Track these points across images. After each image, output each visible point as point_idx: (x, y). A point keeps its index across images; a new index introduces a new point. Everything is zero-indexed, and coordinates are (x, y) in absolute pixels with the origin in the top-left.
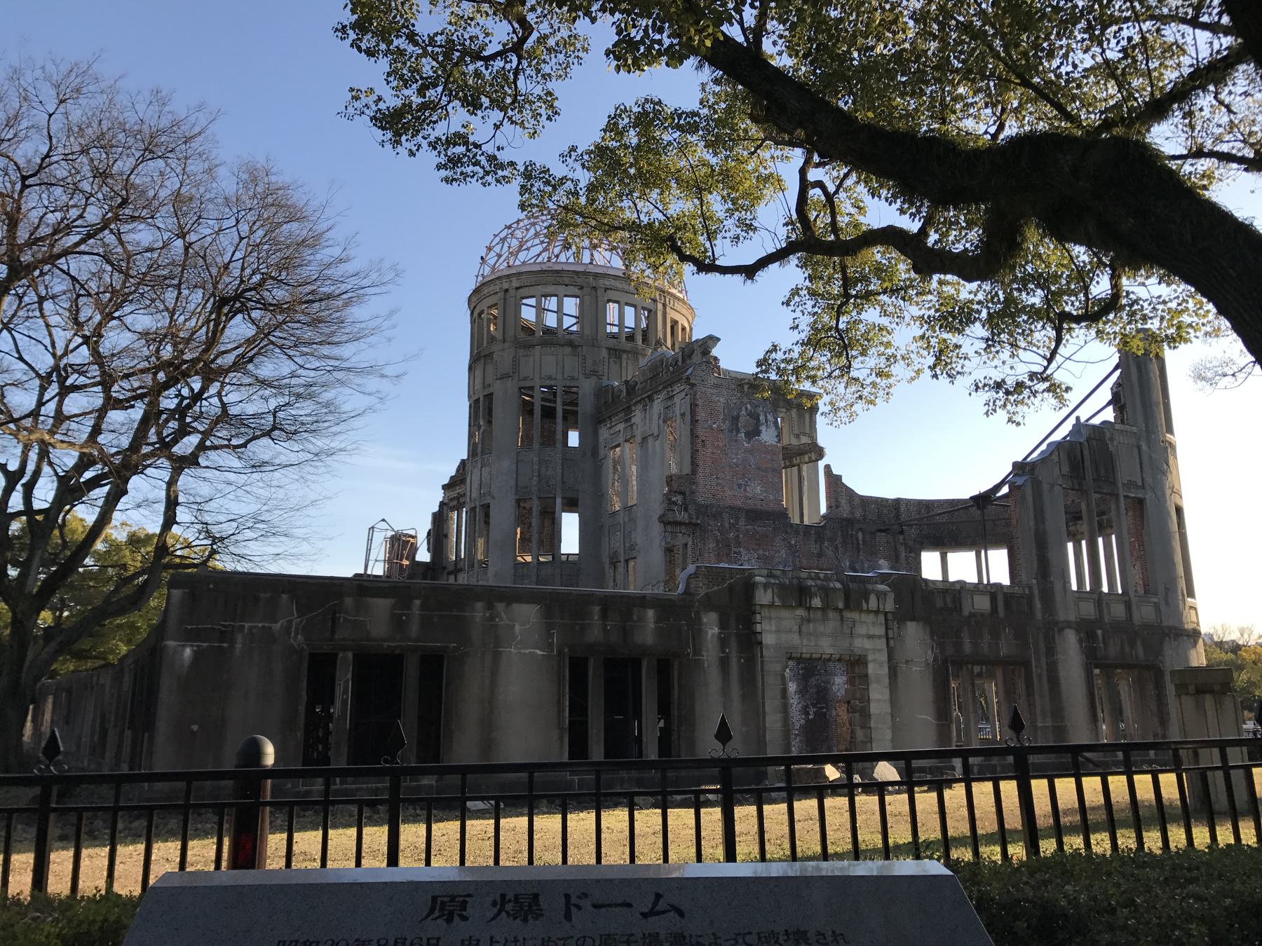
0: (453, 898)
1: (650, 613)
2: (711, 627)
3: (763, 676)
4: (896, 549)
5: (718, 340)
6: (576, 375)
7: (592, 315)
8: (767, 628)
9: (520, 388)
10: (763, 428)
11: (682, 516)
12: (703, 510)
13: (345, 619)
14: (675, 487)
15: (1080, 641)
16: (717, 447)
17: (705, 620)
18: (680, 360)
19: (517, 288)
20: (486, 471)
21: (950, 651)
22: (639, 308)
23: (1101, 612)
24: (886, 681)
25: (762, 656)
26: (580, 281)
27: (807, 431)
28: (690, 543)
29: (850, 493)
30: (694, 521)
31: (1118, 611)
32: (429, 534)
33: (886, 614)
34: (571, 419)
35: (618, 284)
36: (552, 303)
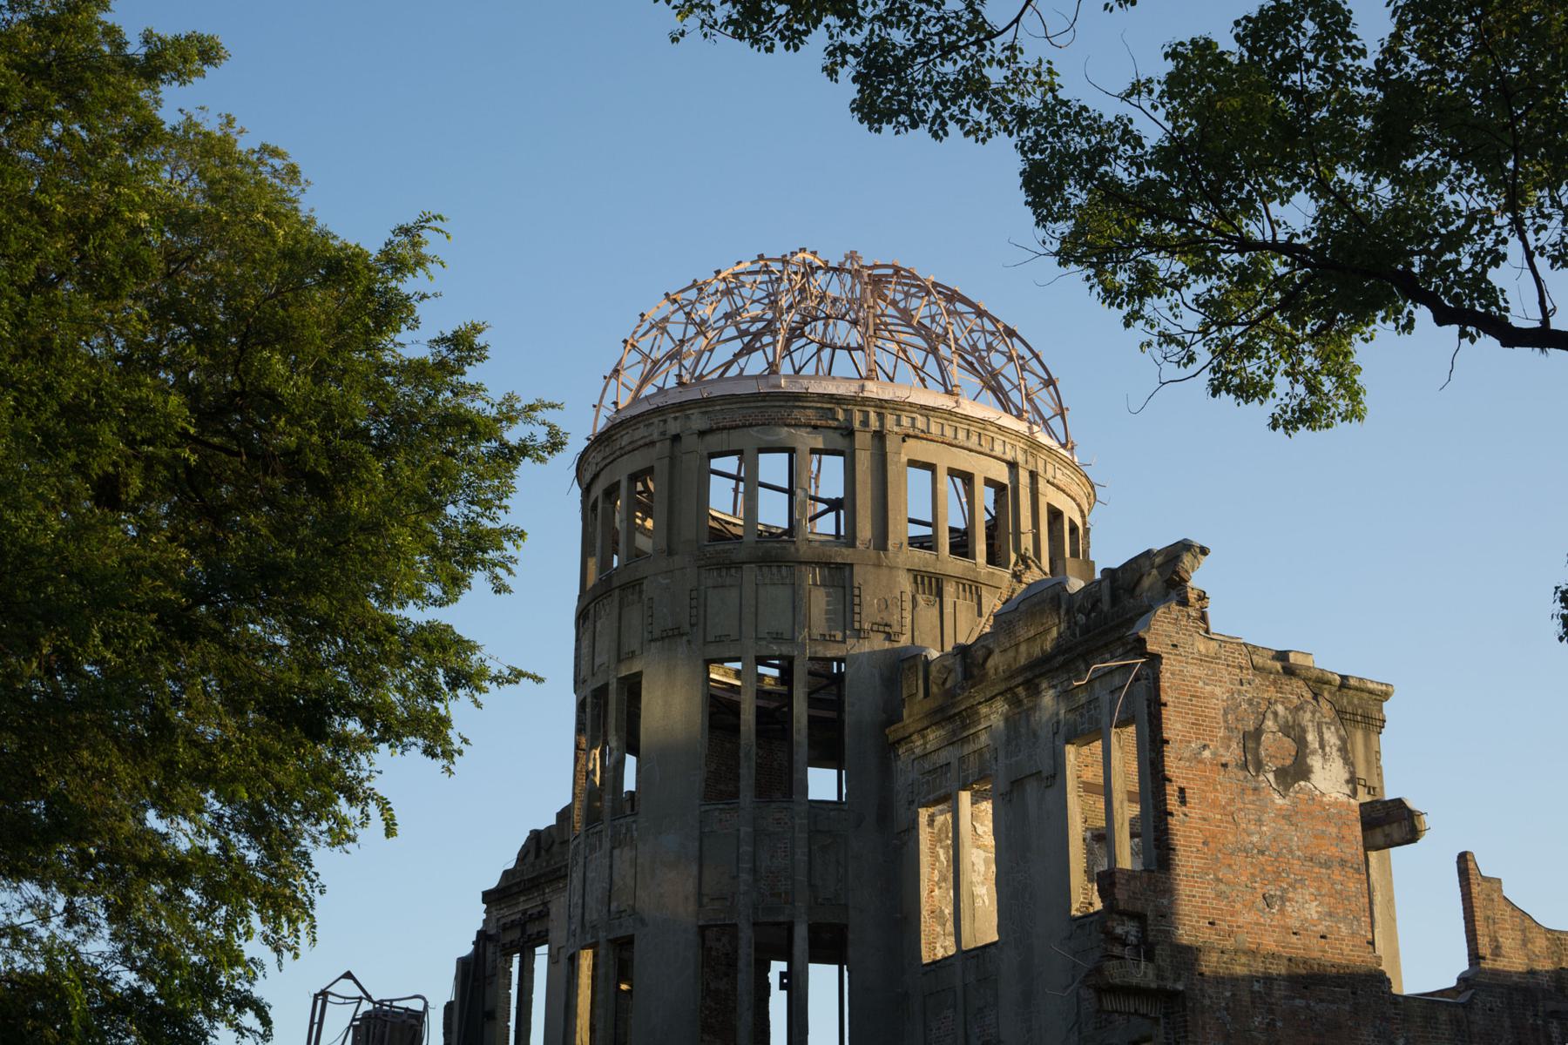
10: (1315, 762)
16: (1214, 804)
18: (1106, 598)
19: (702, 434)
20: (623, 856)
30: (1169, 985)
32: (449, 1007)
36: (773, 467)
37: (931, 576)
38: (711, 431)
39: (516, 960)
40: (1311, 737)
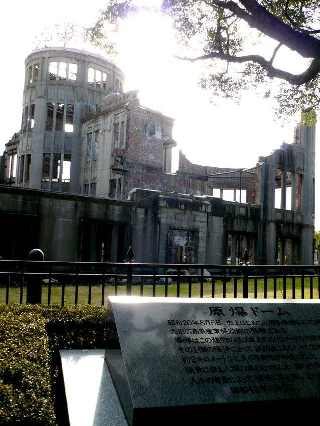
0: (216, 308)
3: (159, 235)
4: (204, 186)
6: (73, 99)
7: (82, 74)
8: (163, 216)
9: (48, 103)
10: (156, 132)
11: (121, 167)
14: (118, 154)
17: (139, 212)
19: (49, 58)
24: (205, 239)
26: (78, 57)
28: (123, 179)
29: (188, 162)
31: (289, 217)
33: (208, 213)
34: (70, 120)
35: (94, 60)
38: (51, 57)
39: (11, 156)
40: (156, 127)
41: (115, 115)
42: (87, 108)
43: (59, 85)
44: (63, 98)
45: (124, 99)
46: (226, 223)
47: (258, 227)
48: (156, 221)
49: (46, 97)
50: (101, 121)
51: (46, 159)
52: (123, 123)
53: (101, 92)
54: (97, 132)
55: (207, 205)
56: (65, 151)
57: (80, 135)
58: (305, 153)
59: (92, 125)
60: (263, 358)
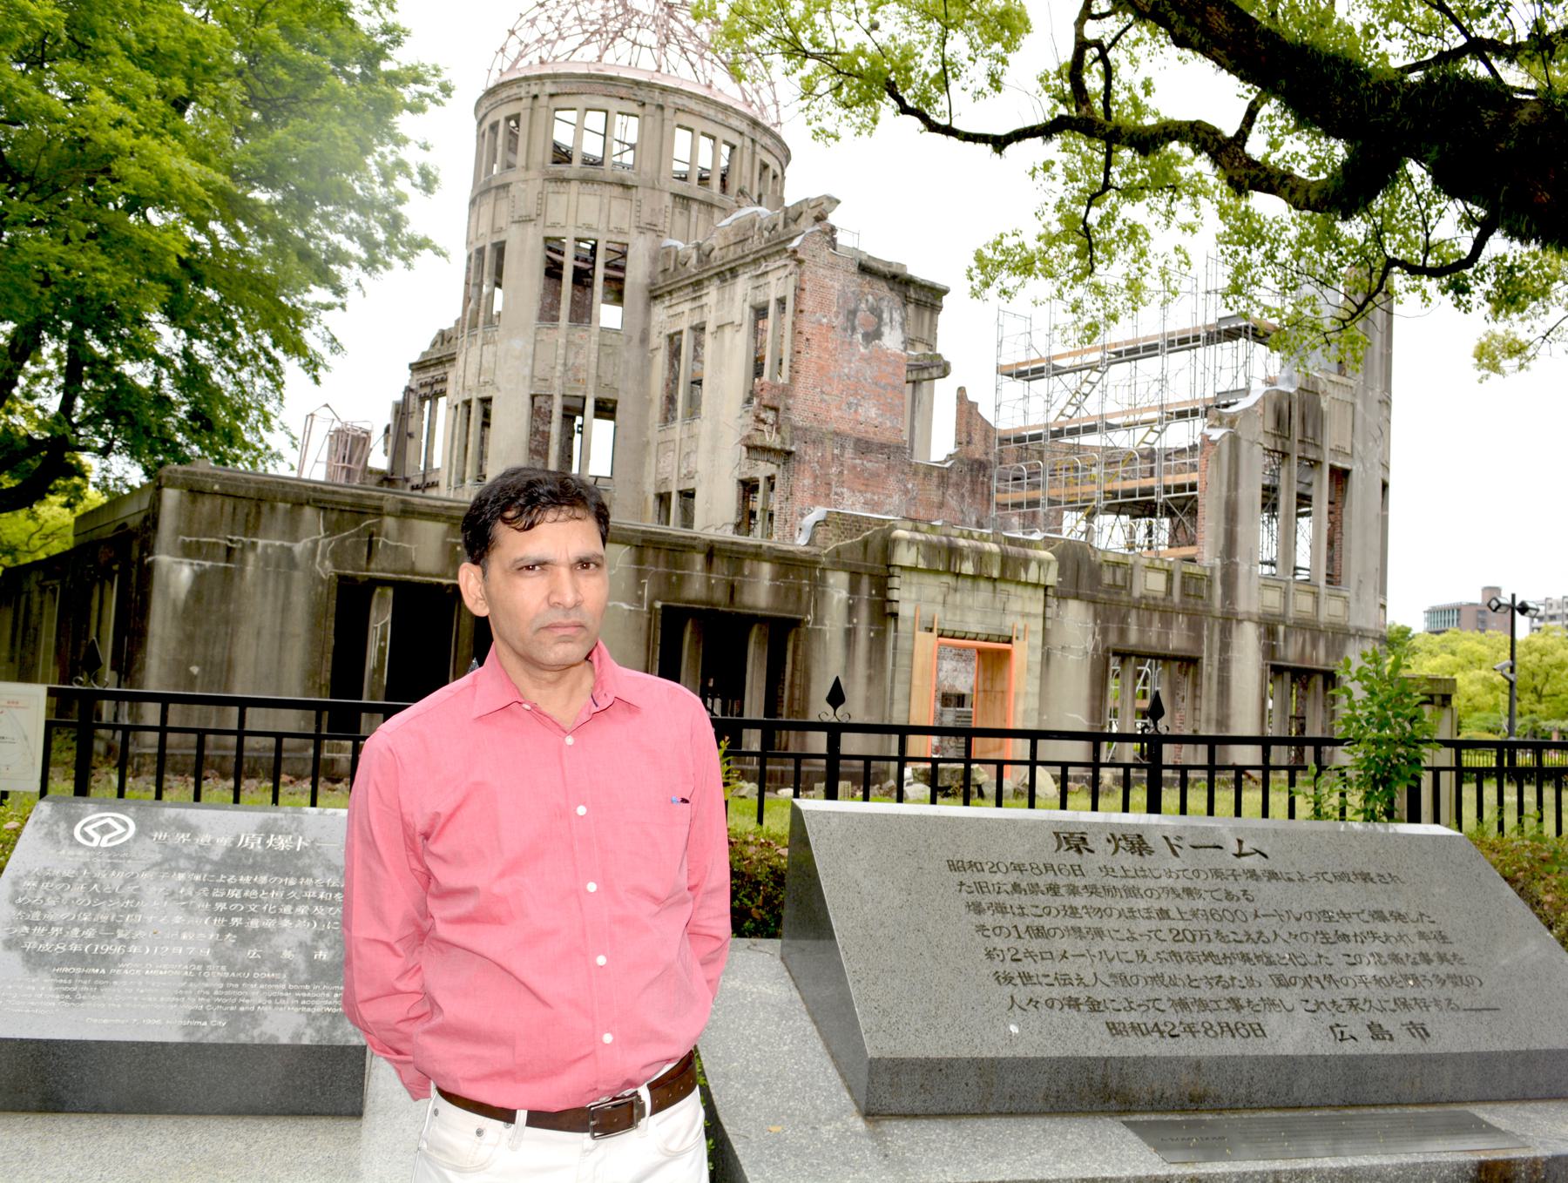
0: (1072, 834)
1: (766, 569)
2: (838, 586)
3: (895, 655)
5: (838, 202)
6: (625, 227)
8: (906, 595)
9: (547, 239)
10: (886, 330)
11: (772, 440)
12: (799, 432)
13: (385, 544)
14: (766, 400)
15: (1260, 638)
16: (826, 349)
18: (781, 224)
19: (552, 95)
21: (1113, 639)
22: (719, 140)
23: (1286, 605)
25: (896, 630)
26: (642, 94)
27: (925, 335)
29: (988, 429)
30: (787, 448)
32: (387, 430)
33: (1046, 588)
35: (692, 104)
37: (684, 198)
39: (427, 403)
40: (886, 316)
41: (758, 276)
42: (668, 254)
43: (585, 180)
44: (594, 222)
45: (786, 225)
46: (1106, 620)
47: (1205, 633)
48: (884, 613)
49: (541, 219)
50: (712, 294)
51: (538, 409)
52: (781, 302)
53: (711, 205)
54: (699, 329)
55: (1041, 563)
56: (598, 385)
57: (644, 339)
58: (1359, 403)
59: (686, 307)
60: (1191, 957)
